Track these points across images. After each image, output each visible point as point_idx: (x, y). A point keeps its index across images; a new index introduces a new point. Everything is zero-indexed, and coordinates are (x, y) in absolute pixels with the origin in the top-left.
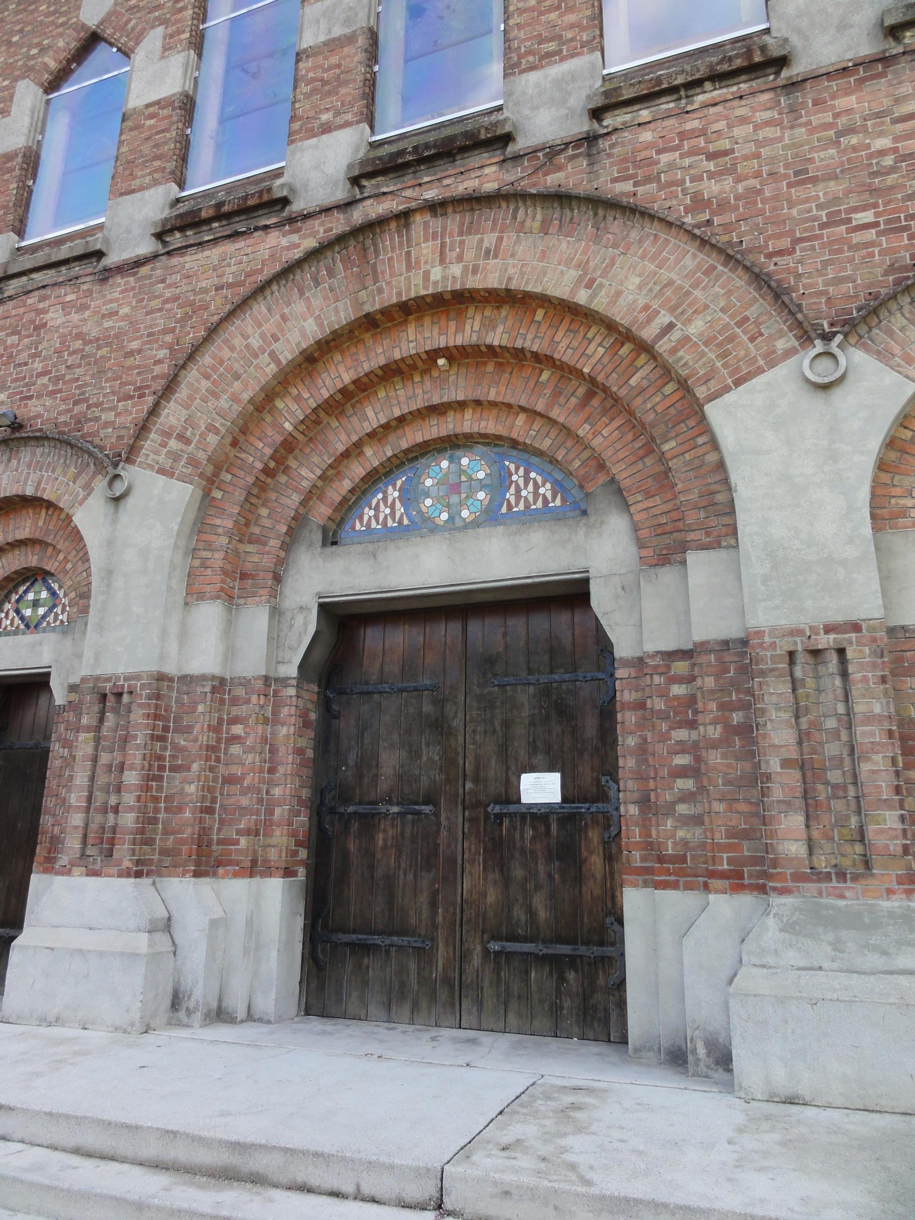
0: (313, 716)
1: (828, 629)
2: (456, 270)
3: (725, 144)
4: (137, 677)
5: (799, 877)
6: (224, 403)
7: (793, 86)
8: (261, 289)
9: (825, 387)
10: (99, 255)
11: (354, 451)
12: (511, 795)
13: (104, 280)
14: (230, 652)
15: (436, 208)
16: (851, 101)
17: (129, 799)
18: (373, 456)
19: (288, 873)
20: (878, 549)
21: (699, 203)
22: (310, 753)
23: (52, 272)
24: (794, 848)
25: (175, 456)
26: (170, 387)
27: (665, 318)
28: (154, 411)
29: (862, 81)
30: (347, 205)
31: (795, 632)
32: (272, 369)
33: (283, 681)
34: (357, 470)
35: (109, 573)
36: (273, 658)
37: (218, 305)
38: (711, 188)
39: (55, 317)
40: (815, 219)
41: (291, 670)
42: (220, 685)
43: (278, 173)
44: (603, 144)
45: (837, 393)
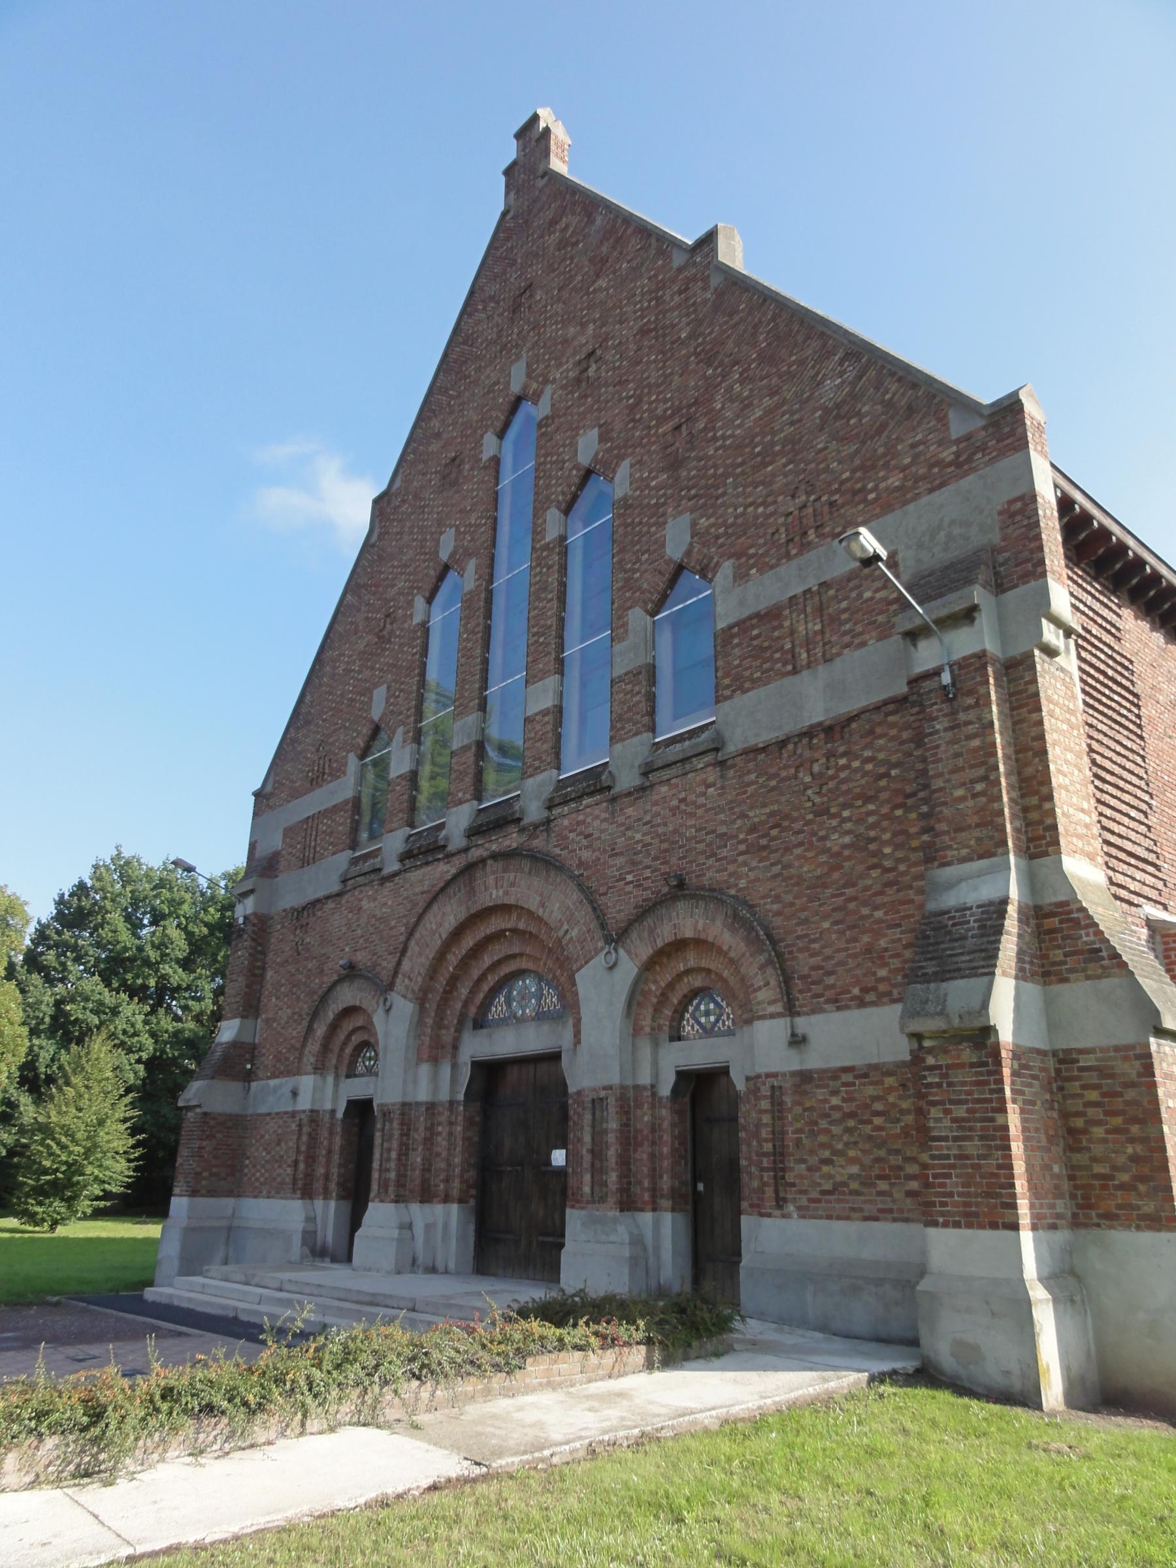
0: (478, 1119)
1: (605, 1088)
2: (501, 892)
3: (590, 830)
4: (393, 1105)
5: (588, 1202)
6: (423, 960)
7: (613, 800)
8: (434, 899)
9: (611, 968)
10: (380, 870)
11: (482, 978)
12: (548, 1162)
13: (382, 884)
14: (436, 1089)
15: (495, 856)
16: (630, 811)
17: (393, 1165)
18: (492, 980)
19: (461, 1201)
20: (633, 1045)
21: (581, 864)
22: (476, 1139)
23: (362, 878)
24: (587, 1189)
25: (407, 987)
26: (404, 952)
27: (566, 927)
28: (399, 963)
29: (636, 799)
30: (466, 850)
31: (594, 1090)
32: (439, 942)
33: (458, 1102)
34: (485, 987)
35: (386, 1048)
36: (453, 1090)
37: (422, 905)
38: (586, 855)
39: (365, 904)
40: (614, 876)
41: (461, 1097)
42: (431, 1107)
43: (442, 826)
44: (552, 824)
45: (615, 970)
